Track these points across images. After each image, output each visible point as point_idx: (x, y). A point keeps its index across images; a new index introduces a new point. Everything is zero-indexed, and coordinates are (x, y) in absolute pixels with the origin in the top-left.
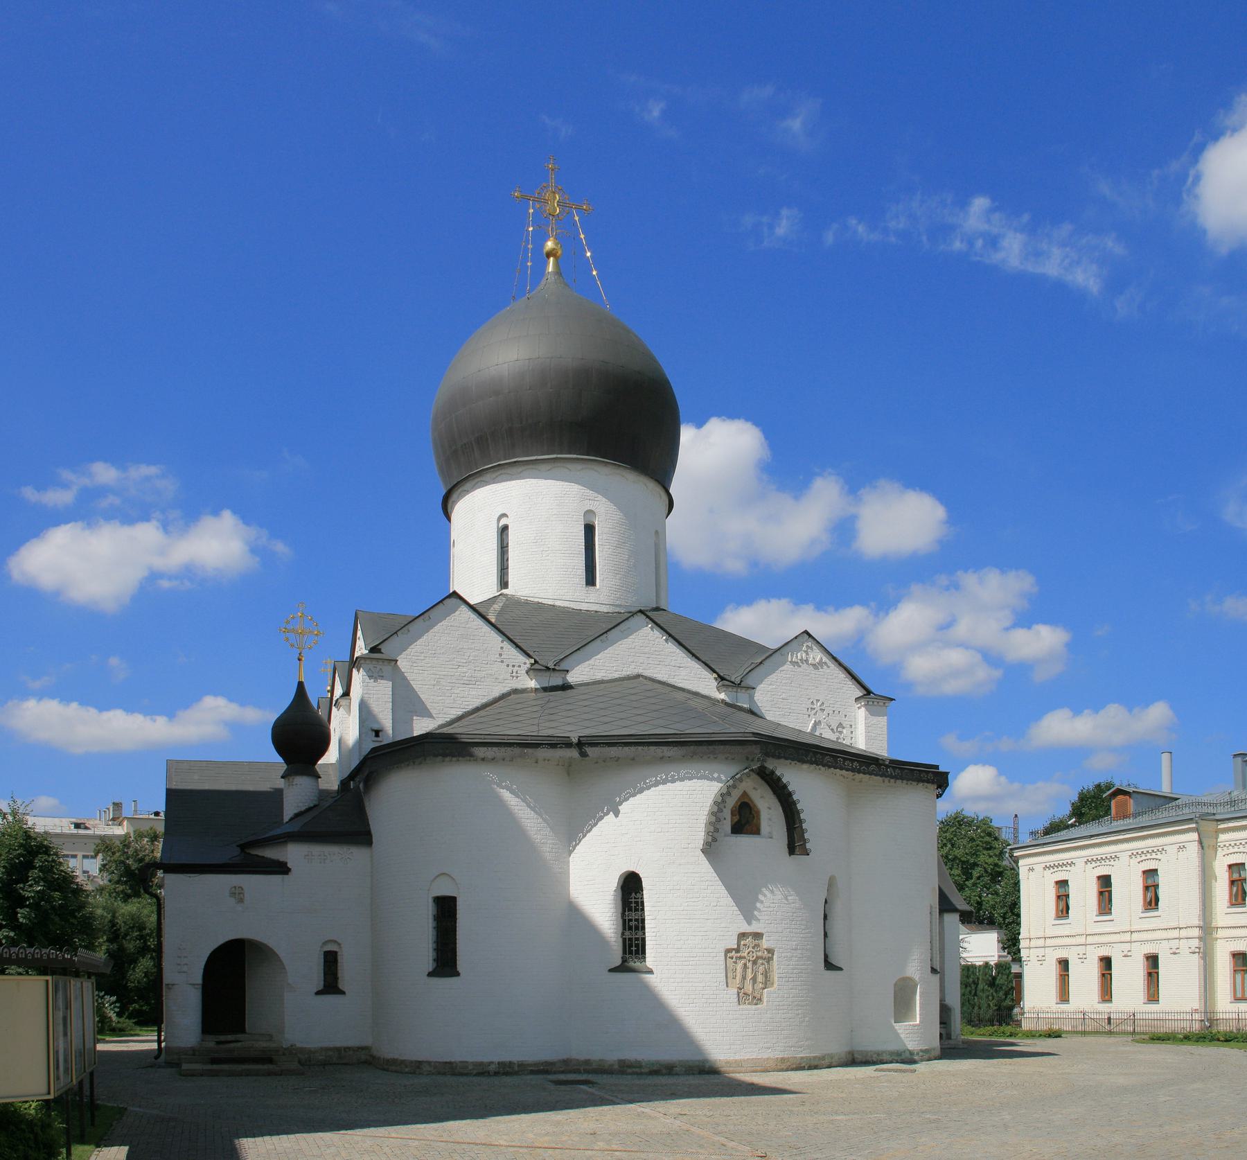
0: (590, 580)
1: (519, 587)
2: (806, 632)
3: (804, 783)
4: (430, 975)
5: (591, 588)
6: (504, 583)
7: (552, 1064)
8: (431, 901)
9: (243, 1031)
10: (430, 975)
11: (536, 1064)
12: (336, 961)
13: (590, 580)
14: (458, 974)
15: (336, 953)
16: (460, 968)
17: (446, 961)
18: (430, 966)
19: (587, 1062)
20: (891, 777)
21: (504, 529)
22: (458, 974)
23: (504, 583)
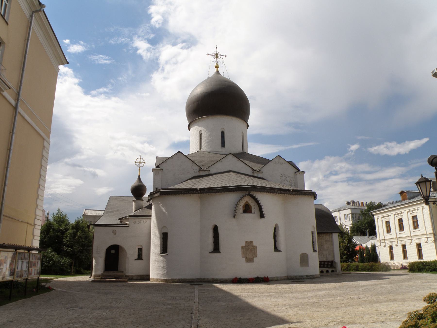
0: (223, 145)
5: (223, 148)
6: (201, 148)
7: (194, 279)
11: (189, 279)
13: (223, 145)
19: (204, 279)
20: (294, 194)
21: (201, 135)
23: (201, 148)
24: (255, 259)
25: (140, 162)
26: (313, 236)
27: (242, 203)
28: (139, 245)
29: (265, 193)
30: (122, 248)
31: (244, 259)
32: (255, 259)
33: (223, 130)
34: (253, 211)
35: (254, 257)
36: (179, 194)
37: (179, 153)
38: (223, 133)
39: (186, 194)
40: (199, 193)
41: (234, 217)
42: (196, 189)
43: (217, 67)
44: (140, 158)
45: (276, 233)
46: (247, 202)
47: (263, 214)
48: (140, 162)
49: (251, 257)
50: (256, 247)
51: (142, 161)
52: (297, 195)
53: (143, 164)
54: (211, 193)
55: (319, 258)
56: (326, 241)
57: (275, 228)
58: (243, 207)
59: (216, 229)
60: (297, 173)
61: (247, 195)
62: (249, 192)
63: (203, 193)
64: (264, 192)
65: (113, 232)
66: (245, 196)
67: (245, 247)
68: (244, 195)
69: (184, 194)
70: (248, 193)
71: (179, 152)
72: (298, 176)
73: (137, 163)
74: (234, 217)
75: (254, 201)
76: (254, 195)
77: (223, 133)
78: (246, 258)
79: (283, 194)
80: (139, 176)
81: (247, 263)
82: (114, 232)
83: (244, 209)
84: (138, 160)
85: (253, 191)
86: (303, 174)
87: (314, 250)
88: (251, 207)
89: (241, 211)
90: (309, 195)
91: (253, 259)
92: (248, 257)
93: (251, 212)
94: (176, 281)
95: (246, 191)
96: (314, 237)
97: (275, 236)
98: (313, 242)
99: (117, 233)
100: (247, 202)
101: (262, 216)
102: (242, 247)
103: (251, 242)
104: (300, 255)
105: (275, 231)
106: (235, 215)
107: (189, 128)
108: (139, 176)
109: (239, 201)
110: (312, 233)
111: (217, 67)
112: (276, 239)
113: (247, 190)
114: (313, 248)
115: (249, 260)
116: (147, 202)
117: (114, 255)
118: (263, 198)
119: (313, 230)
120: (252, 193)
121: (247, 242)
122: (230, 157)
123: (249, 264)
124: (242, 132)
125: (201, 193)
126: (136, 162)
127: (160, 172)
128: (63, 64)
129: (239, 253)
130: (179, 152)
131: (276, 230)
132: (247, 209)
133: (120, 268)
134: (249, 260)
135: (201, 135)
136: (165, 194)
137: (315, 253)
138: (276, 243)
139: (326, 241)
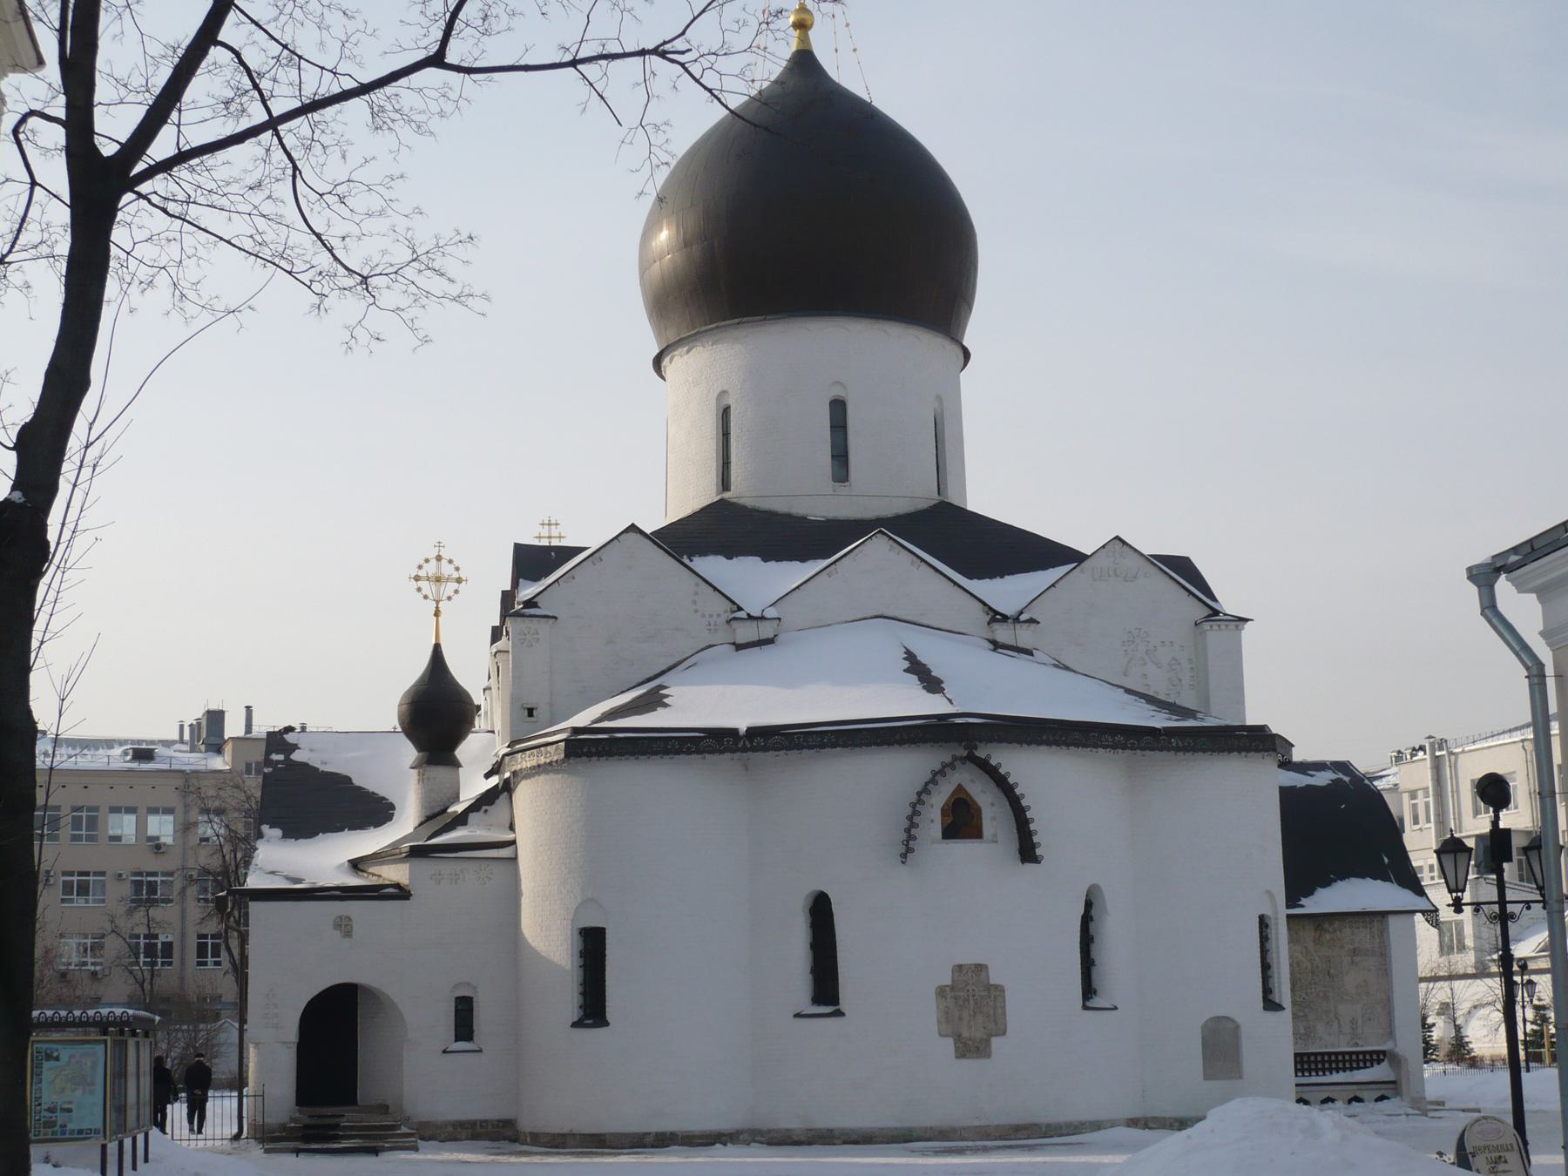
1: (743, 491)
2: (1117, 538)
3: (1027, 768)
4: (574, 1025)
5: (842, 489)
8: (576, 933)
9: (354, 1102)
10: (574, 1025)
12: (471, 1010)
14: (606, 1024)
15: (470, 999)
16: (610, 1014)
17: (593, 1010)
18: (575, 1014)
20: (1177, 749)
21: (725, 413)
22: (606, 1024)
23: (725, 484)
24: (994, 1040)
25: (438, 580)
26: (1264, 939)
27: (940, 797)
28: (456, 986)
29: (1044, 748)
30: (370, 992)
31: (949, 1044)
32: (994, 1040)
33: (837, 392)
34: (988, 827)
35: (991, 1035)
36: (655, 753)
37: (632, 536)
38: (838, 409)
39: (689, 752)
40: (744, 750)
41: (904, 856)
42: (733, 732)
43: (802, 26)
44: (439, 558)
45: (1092, 926)
46: (960, 788)
47: (1033, 846)
48: (438, 580)
49: (979, 1034)
50: (1000, 989)
51: (447, 570)
52: (1195, 750)
53: (453, 586)
54: (800, 747)
55: (1297, 1036)
56: (1354, 952)
57: (1089, 905)
58: (944, 812)
59: (821, 911)
60: (1206, 626)
61: (963, 760)
62: (971, 748)
63: (765, 749)
64: (1039, 743)
65: (337, 926)
66: (951, 766)
67: (952, 988)
68: (948, 759)
69: (678, 752)
70: (965, 753)
71: (633, 528)
72: (1215, 636)
73: (423, 584)
74: (904, 856)
75: (993, 784)
76: (993, 762)
77: (838, 409)
78: (958, 1038)
79: (1124, 748)
80: (437, 648)
81: (965, 1062)
82: (344, 926)
83: (949, 820)
84: (431, 569)
85: (990, 740)
86: (1239, 629)
87: (1271, 1004)
88: (979, 810)
89: (936, 829)
90: (1248, 750)
91: (987, 1042)
92: (965, 1034)
93: (975, 833)
94: (649, 1140)
95: (959, 741)
96: (1272, 945)
97: (1087, 940)
98: (1266, 967)
99: (356, 930)
100: (960, 788)
101: (1028, 852)
102: (941, 992)
103: (980, 968)
104: (1204, 1027)
105: (1087, 920)
106: (909, 850)
107: (658, 363)
108: (437, 648)
109: (925, 790)
110: (1263, 922)
111: (802, 26)
112: (1094, 955)
113: (964, 738)
114: (1267, 991)
115: (972, 1048)
116: (487, 776)
117: (335, 1029)
118: (1027, 768)
119: (1267, 911)
120: (981, 753)
121: (960, 966)
122: (877, 551)
123: (971, 1065)
124: (939, 398)
125: (754, 749)
126: (417, 578)
127: (543, 627)
128: (18, 67)
129: (928, 1013)
130: (633, 528)
131: (1093, 912)
132: (962, 822)
133: (367, 1089)
134: (972, 1048)
135: (725, 413)
136: (589, 755)
137: (1271, 1015)
138: (1095, 971)
139: (1354, 952)
